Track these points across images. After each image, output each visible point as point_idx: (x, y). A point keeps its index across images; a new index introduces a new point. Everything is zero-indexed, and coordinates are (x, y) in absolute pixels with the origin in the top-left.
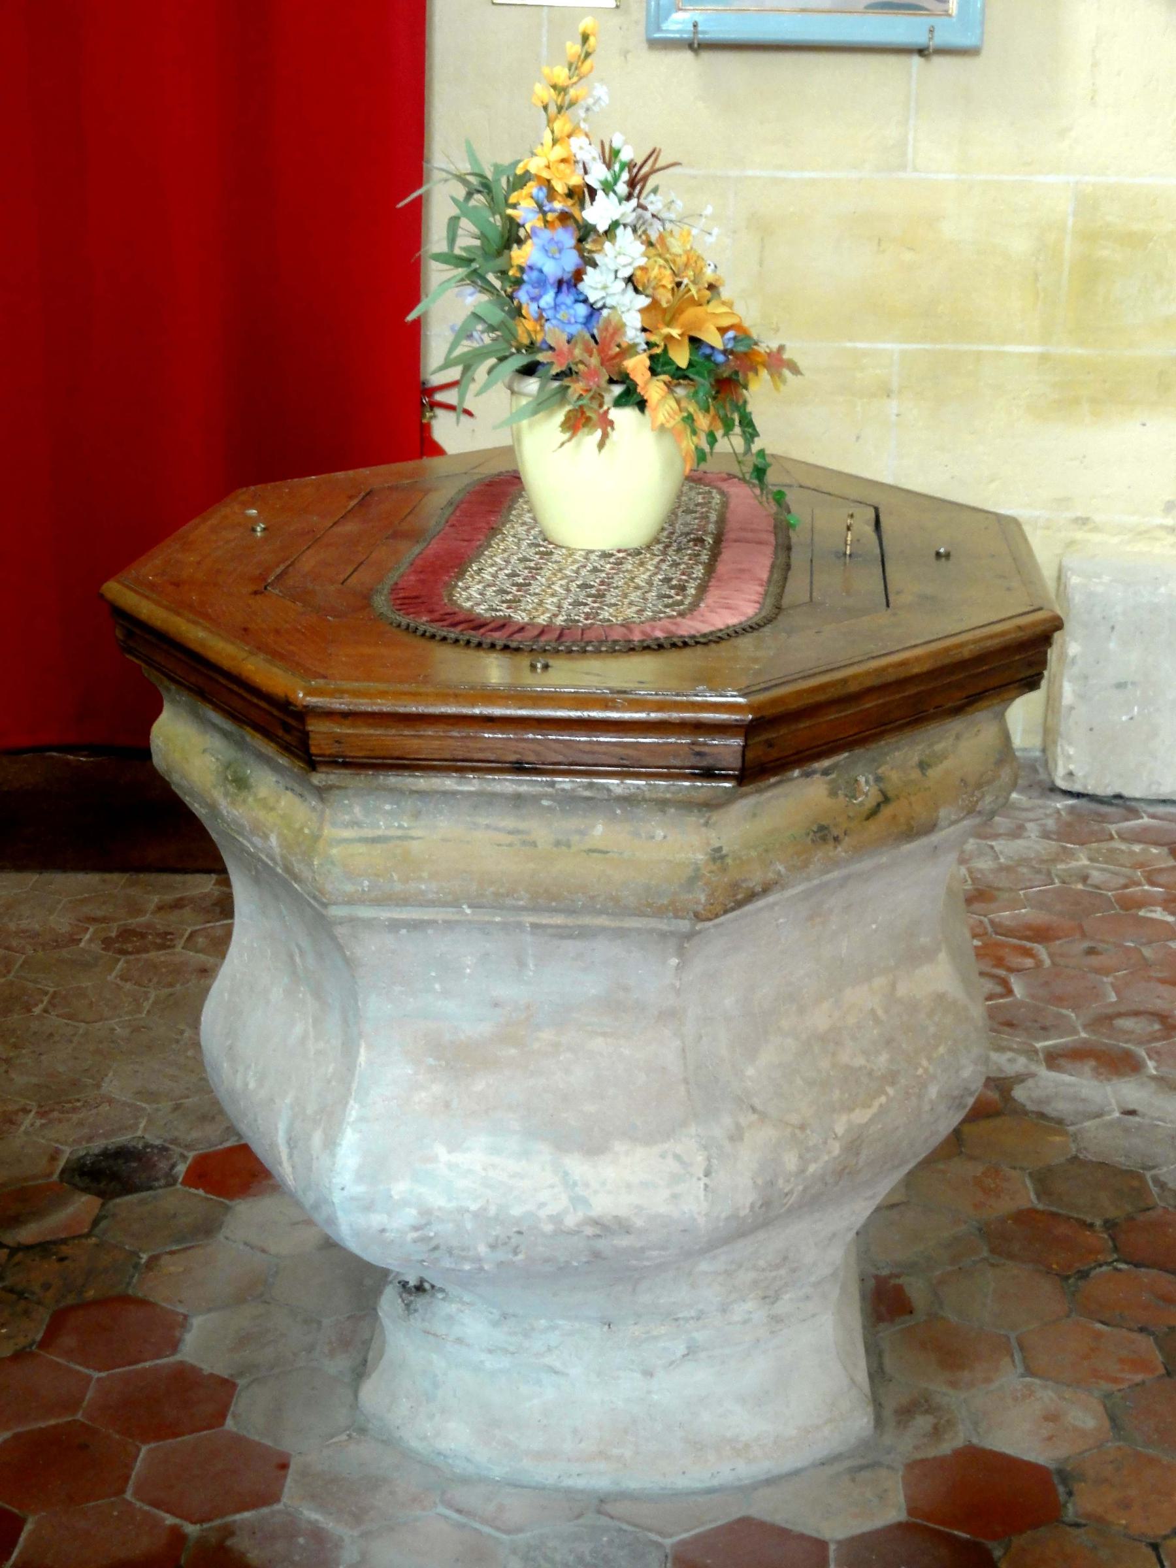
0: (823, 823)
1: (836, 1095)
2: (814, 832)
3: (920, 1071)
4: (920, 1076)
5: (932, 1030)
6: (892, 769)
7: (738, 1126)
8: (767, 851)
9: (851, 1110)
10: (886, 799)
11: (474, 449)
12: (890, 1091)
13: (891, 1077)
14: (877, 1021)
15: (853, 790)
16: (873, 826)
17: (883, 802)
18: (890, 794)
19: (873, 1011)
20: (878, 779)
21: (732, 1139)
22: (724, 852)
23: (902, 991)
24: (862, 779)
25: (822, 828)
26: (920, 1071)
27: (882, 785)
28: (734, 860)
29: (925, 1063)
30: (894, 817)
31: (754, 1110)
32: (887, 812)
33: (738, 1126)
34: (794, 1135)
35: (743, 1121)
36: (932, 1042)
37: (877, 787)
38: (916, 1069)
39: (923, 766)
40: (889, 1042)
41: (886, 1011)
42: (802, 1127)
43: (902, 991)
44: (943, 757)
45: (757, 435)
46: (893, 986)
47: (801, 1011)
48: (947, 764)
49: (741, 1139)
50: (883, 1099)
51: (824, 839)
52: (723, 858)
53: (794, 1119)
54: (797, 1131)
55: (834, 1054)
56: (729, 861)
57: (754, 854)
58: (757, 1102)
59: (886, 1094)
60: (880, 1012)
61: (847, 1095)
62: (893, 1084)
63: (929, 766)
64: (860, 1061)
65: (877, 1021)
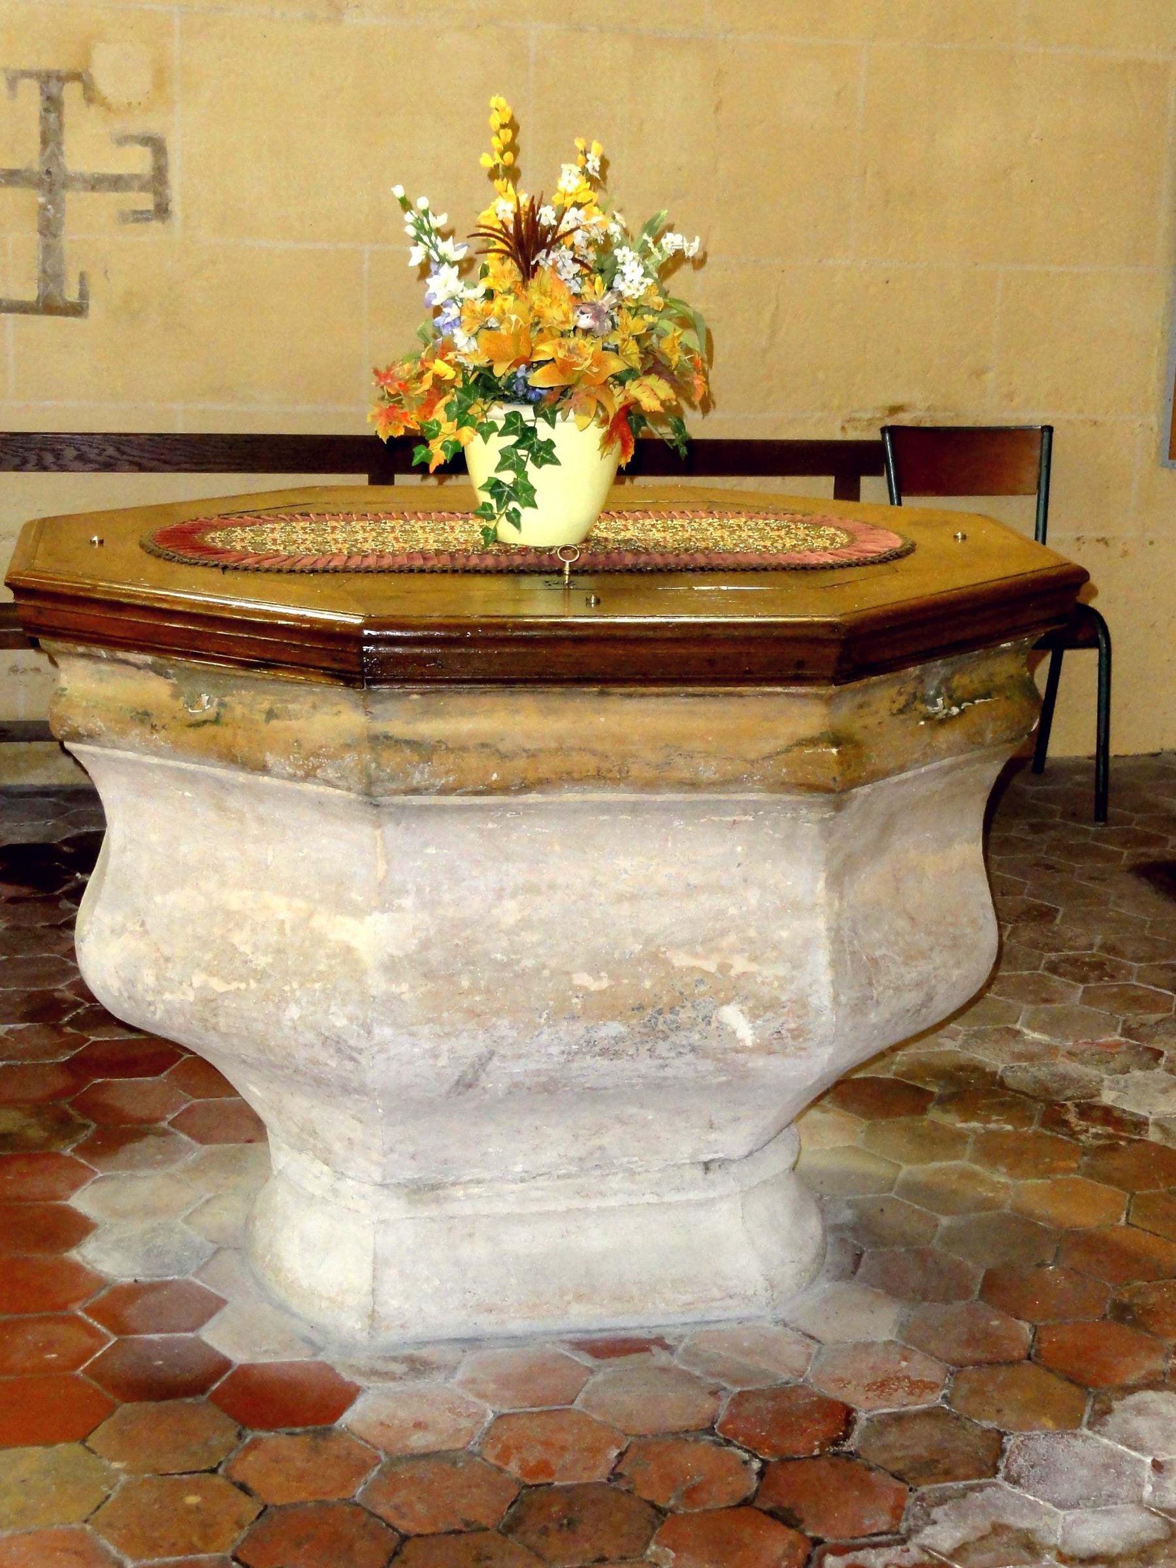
0: (150, 711)
1: (209, 956)
2: (138, 713)
3: (287, 988)
4: (286, 992)
5: (322, 967)
6: (240, 703)
7: (124, 926)
8: (94, 707)
9: (211, 974)
10: (217, 721)
11: (1057, 701)
12: (253, 984)
13: (261, 976)
14: (282, 931)
15: (193, 702)
16: (192, 734)
17: (211, 721)
18: (223, 720)
19: (283, 922)
20: (222, 704)
21: (113, 931)
22: (66, 692)
23: (318, 922)
24: (205, 698)
25: (146, 714)
26: (287, 988)
27: (222, 711)
28: (68, 700)
29: (295, 985)
30: (214, 737)
31: (143, 924)
32: (210, 730)
33: (124, 926)
34: (157, 960)
35: (130, 926)
36: (314, 975)
37: (216, 710)
38: (286, 984)
39: (271, 715)
40: (279, 952)
41: (293, 929)
42: (167, 960)
43: (318, 922)
44: (290, 716)
45: (535, 490)
46: (311, 915)
47: (223, 884)
48: (294, 724)
49: (120, 936)
50: (243, 986)
51: (142, 722)
52: (61, 695)
53: (167, 951)
54: (162, 961)
55: (229, 931)
56: (63, 699)
57: (84, 704)
58: (149, 922)
59: (248, 984)
60: (288, 927)
61: (216, 963)
62: (259, 981)
63: (277, 717)
64: (246, 949)
65: (282, 931)
